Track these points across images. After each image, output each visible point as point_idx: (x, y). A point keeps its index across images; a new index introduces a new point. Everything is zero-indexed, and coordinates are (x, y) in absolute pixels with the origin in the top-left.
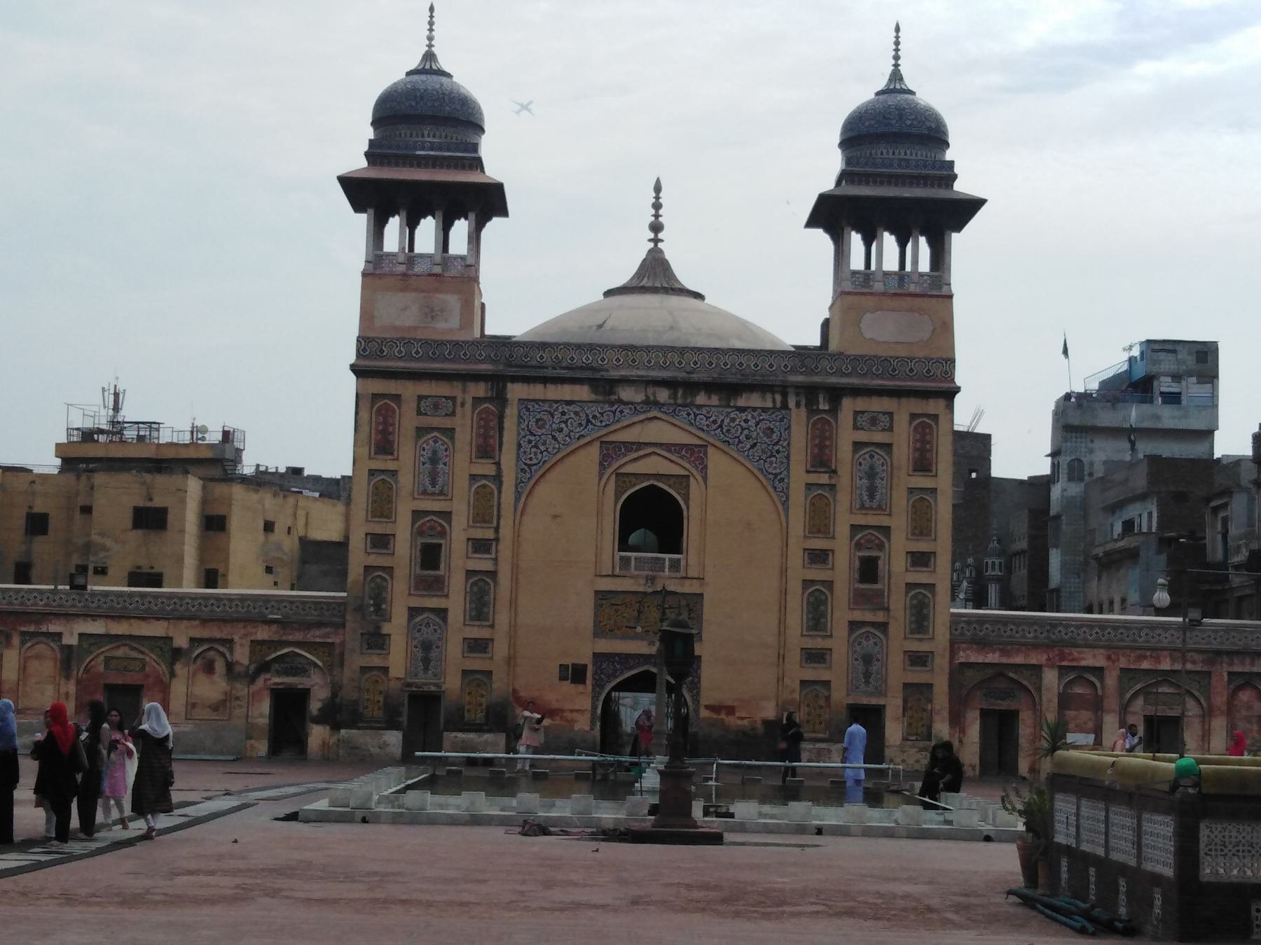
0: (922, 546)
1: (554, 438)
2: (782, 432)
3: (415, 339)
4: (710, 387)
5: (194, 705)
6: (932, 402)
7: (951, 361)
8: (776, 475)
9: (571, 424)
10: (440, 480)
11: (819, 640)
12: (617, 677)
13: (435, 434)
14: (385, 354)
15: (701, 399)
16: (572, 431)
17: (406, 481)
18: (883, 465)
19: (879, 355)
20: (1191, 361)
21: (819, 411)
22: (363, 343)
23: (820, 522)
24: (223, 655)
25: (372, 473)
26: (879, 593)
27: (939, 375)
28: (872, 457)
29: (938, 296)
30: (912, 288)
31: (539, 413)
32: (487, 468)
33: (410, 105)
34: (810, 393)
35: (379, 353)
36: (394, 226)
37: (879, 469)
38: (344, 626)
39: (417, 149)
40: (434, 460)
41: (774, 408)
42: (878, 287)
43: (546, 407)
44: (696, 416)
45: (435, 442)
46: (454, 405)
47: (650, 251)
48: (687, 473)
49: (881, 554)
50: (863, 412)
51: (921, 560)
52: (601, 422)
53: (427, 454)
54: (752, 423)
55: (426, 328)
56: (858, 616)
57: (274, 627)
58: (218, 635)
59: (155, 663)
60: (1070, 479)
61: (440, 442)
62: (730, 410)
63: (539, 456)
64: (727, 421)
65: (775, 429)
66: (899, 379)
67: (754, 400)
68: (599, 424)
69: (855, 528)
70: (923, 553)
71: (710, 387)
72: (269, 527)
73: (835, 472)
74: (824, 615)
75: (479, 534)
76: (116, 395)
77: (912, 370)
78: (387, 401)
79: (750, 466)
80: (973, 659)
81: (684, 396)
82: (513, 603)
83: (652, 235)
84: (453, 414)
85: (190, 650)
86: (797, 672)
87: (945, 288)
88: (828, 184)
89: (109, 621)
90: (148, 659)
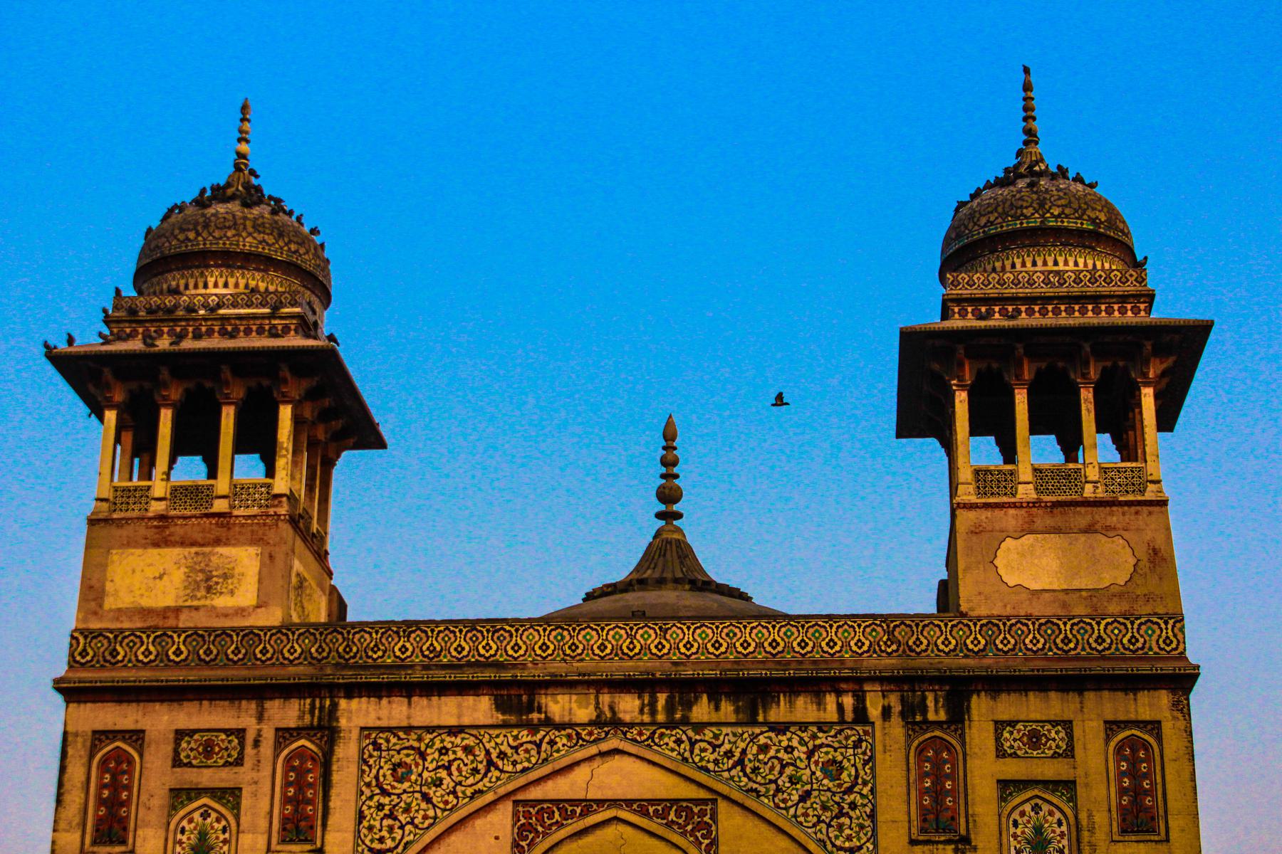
1: (426, 798)
2: (859, 766)
3: (175, 629)
4: (716, 688)
6: (1143, 697)
7: (1178, 619)
9: (459, 770)
13: (205, 800)
14: (120, 658)
15: (702, 710)
16: (460, 783)
18: (1060, 823)
21: (927, 725)
22: (82, 640)
27: (1156, 649)
28: (1036, 808)
29: (1140, 503)
30: (1088, 491)
31: (399, 752)
33: (187, 239)
35: (109, 658)
41: (842, 721)
44: (693, 744)
45: (205, 816)
50: (1012, 723)
52: (514, 763)
54: (800, 752)
55: (197, 608)
61: (214, 815)
62: (757, 731)
63: (398, 834)
65: (845, 763)
67: (804, 709)
68: (510, 768)
71: (716, 688)
73: (966, 840)
77: (1100, 640)
78: (119, 744)
79: (802, 838)
81: (670, 708)
83: (662, 507)
84: (239, 762)
87: (1151, 487)
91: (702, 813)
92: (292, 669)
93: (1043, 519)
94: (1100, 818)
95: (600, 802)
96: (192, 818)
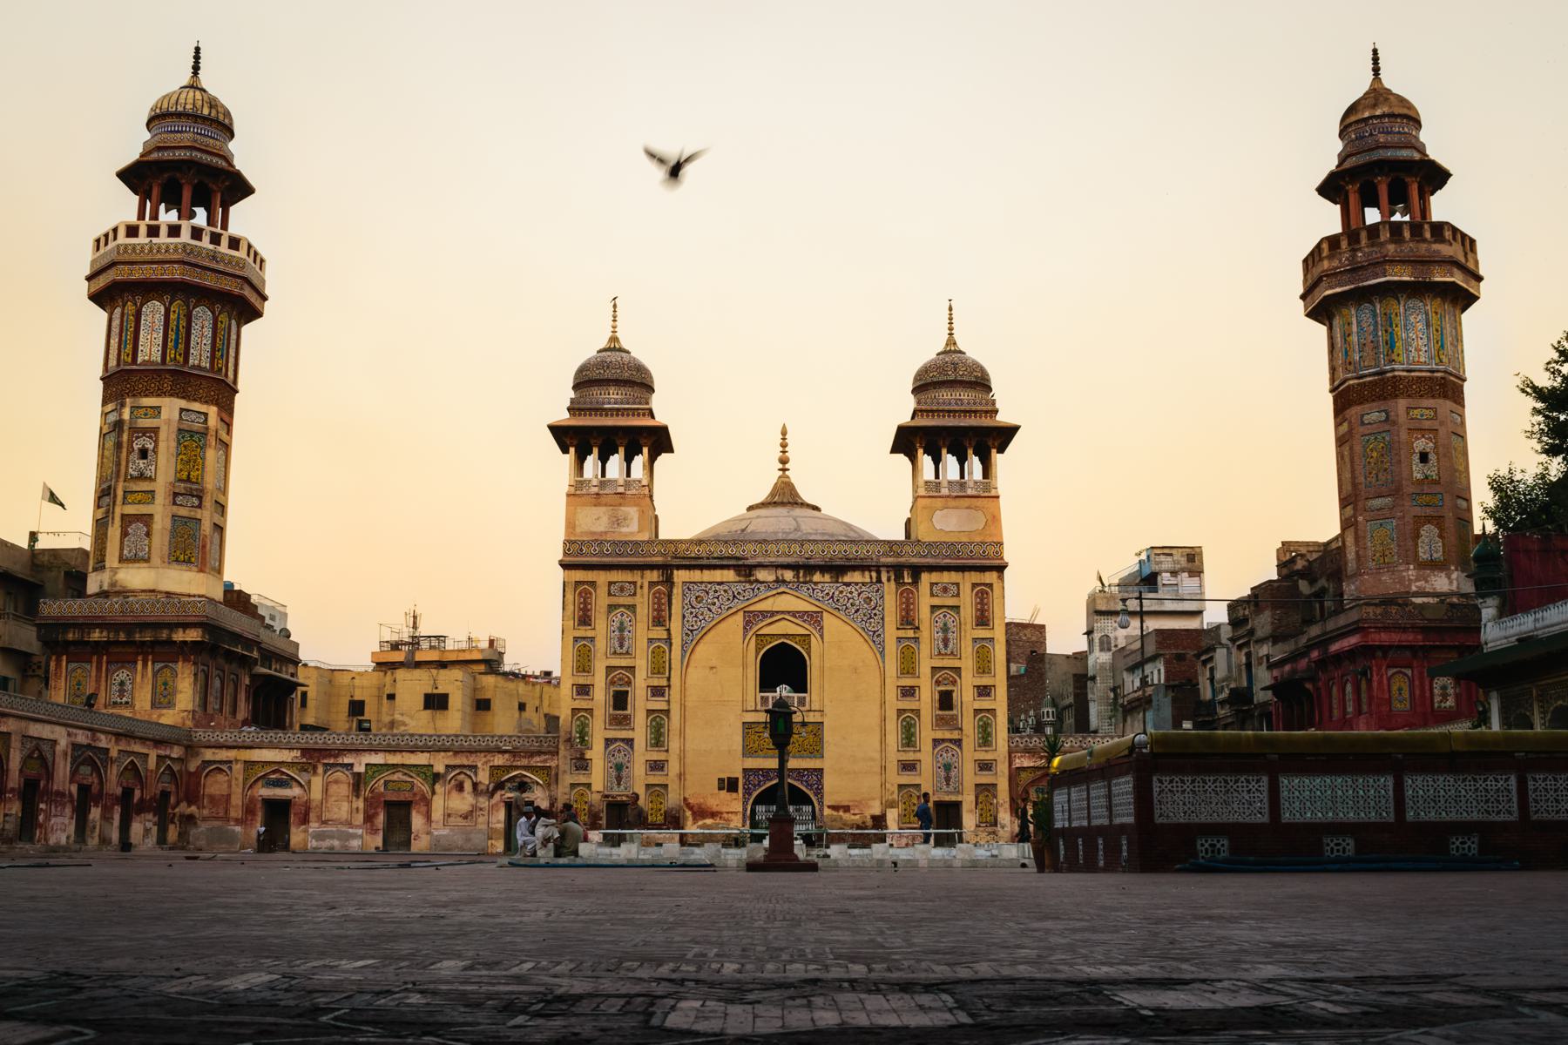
0: (985, 681)
5: (449, 815)
6: (987, 574)
7: (1002, 544)
8: (874, 632)
10: (626, 644)
11: (911, 753)
12: (761, 787)
13: (622, 609)
15: (817, 577)
17: (601, 645)
19: (947, 540)
20: (1183, 561)
21: (904, 583)
23: (908, 665)
24: (470, 777)
25: (576, 639)
26: (954, 718)
28: (945, 616)
30: (970, 492)
32: (660, 633)
34: (897, 570)
36: (591, 462)
37: (950, 624)
38: (558, 753)
39: (604, 403)
40: (621, 629)
42: (945, 491)
43: (703, 587)
44: (813, 590)
45: (622, 615)
46: (635, 587)
47: (780, 477)
48: (807, 632)
49: (955, 689)
50: (937, 584)
51: (984, 691)
53: (617, 624)
54: (855, 594)
56: (939, 735)
57: (507, 756)
58: (466, 762)
59: (422, 786)
60: (1101, 650)
64: (837, 593)
66: (963, 559)
67: (856, 577)
69: (934, 669)
70: (985, 687)
71: (824, 569)
72: (522, 707)
73: (918, 628)
74: (913, 735)
75: (656, 682)
76: (415, 617)
77: (971, 551)
80: (1025, 765)
81: (805, 576)
82: (682, 733)
83: (781, 466)
84: (635, 594)
85: (444, 776)
86: (896, 778)
88: (905, 418)
89: (387, 754)
90: (415, 781)
91: (817, 617)
92: (654, 559)
93: (952, 503)
94: (969, 620)
95: (777, 612)
96: (617, 617)
